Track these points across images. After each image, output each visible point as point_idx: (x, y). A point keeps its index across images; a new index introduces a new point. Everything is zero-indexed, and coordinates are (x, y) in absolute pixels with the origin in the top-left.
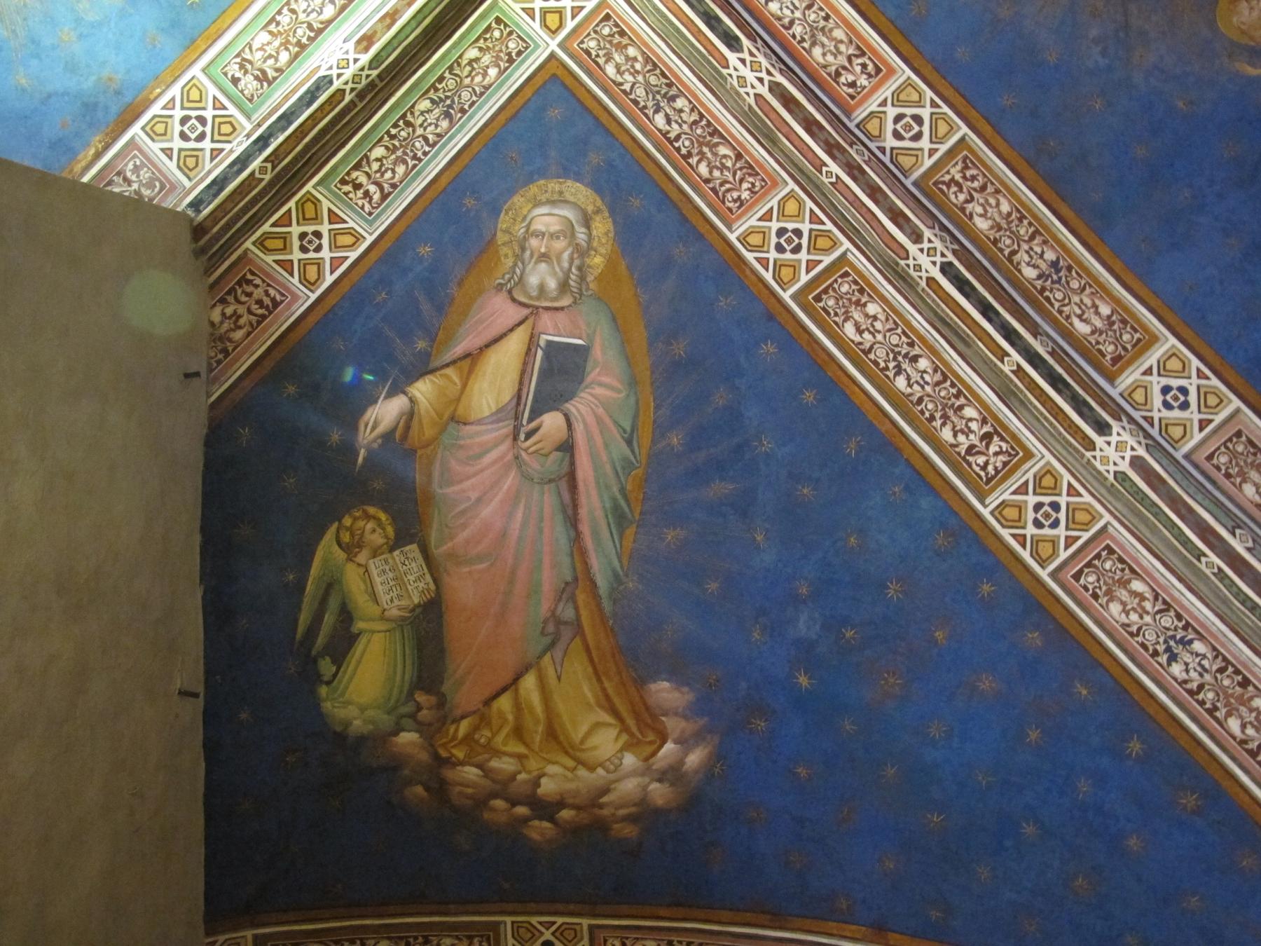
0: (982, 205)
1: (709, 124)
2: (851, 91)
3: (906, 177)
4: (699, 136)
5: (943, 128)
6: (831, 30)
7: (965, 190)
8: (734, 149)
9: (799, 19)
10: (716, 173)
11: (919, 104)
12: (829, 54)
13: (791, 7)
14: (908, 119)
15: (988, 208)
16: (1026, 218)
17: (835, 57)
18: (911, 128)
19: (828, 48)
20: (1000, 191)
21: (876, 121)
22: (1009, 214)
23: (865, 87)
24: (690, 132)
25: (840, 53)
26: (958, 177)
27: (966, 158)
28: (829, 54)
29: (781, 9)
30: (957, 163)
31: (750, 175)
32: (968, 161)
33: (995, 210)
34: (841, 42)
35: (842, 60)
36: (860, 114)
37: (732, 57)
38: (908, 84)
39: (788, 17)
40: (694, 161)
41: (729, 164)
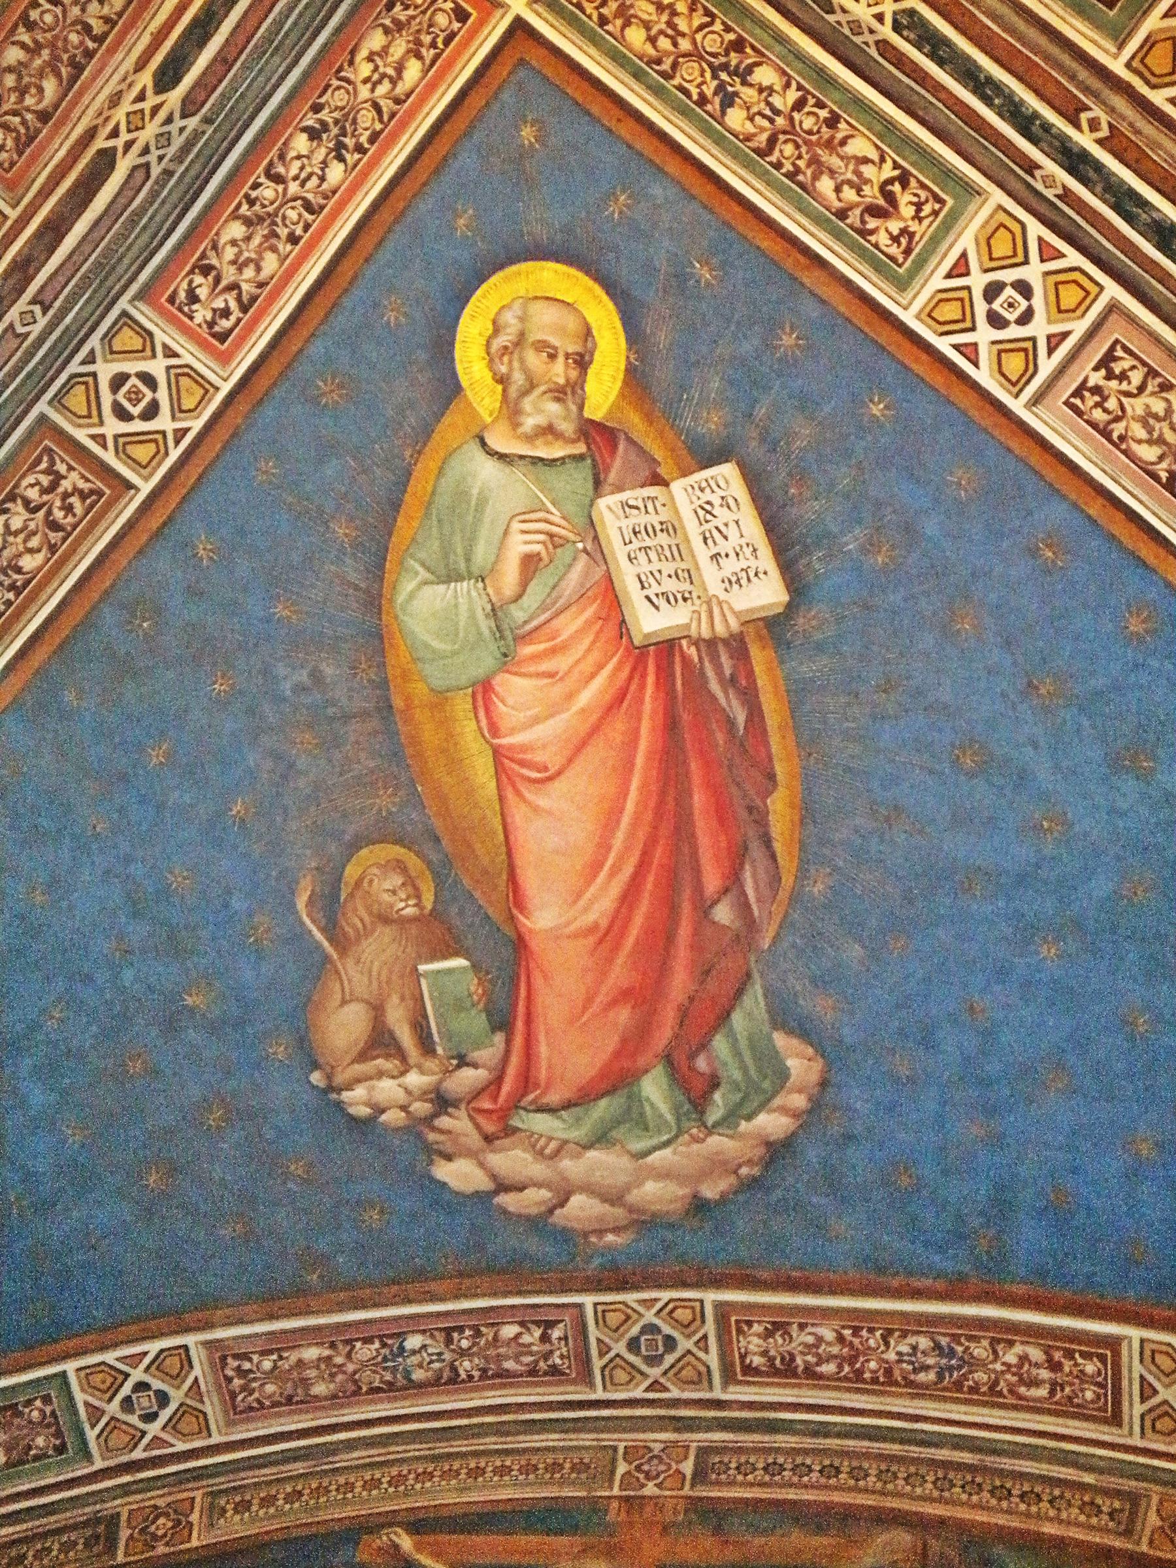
0: (25, 527)
1: (89, 54)
2: (182, 295)
3: (50, 403)
4: (66, 40)
5: (142, 453)
6: (274, 249)
7: (45, 498)
8: (56, 106)
9: (285, 190)
10: (10, 80)
11: (178, 410)
12: (236, 250)
13: (303, 175)
14: (149, 395)
15: (22, 536)
16: (18, 595)
17: (234, 262)
18: (136, 402)
19: (244, 247)
20: (53, 554)
21: (137, 343)
22: (19, 570)
23: (191, 318)
24: (69, 21)
25: (240, 270)
26: (66, 485)
27: (100, 494)
28: (236, 250)
29: (299, 157)
30: (87, 480)
31: (17, 139)
32: (94, 497)
33: (21, 548)
34: (258, 269)
35: (229, 274)
36: (144, 315)
37: (146, 78)
38: (207, 388)
39: (287, 171)
40: (24, 37)
41: (29, 101)
